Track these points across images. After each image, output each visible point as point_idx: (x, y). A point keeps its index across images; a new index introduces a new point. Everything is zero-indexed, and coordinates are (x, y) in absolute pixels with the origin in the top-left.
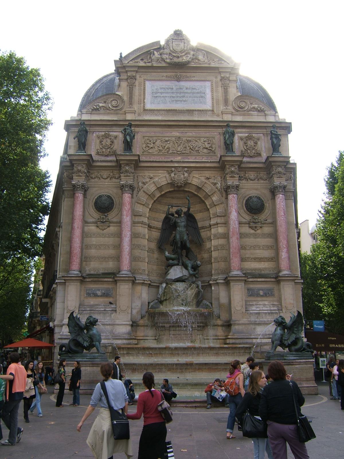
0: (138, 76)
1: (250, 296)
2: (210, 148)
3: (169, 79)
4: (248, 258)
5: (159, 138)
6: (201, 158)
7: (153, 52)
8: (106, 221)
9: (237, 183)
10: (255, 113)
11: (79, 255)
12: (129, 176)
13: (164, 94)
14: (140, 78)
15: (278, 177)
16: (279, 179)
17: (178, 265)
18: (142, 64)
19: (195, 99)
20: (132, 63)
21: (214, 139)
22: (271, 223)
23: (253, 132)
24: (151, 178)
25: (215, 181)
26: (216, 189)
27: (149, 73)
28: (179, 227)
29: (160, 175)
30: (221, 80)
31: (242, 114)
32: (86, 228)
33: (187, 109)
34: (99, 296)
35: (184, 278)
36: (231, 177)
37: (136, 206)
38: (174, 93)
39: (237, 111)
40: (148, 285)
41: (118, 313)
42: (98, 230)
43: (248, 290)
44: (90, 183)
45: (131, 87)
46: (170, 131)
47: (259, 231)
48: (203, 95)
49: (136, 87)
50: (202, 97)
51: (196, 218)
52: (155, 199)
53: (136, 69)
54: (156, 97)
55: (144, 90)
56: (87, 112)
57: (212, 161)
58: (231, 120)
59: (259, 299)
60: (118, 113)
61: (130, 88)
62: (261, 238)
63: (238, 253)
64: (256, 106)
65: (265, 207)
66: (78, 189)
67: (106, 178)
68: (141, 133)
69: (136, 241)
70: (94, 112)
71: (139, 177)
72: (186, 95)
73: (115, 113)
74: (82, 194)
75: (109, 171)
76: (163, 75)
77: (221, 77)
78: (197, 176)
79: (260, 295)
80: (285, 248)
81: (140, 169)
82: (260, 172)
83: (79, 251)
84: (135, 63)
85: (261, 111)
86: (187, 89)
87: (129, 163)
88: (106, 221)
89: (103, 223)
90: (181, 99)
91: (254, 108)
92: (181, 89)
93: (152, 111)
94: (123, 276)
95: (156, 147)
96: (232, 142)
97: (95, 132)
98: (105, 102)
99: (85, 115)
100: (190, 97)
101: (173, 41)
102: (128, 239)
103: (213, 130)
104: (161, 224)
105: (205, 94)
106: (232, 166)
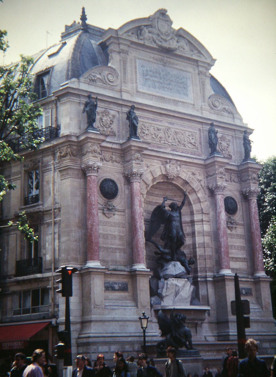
2: (195, 144)
5: (153, 125)
6: (187, 152)
14: (133, 54)
24: (148, 167)
28: (175, 221)
47: (234, 232)
48: (185, 86)
62: (236, 238)
64: (227, 107)
70: (92, 82)
88: (112, 209)
98: (100, 74)
99: (83, 84)
101: (159, 20)
106: (221, 167)
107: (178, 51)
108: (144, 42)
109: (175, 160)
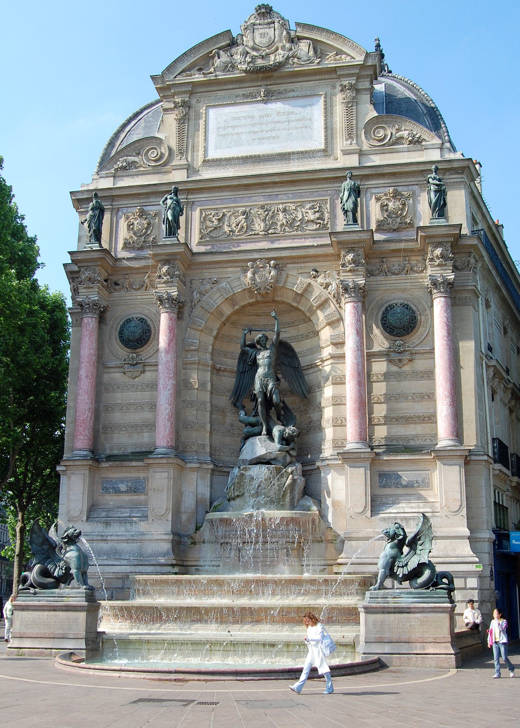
0: (194, 101)
1: (384, 487)
8: (137, 364)
11: (90, 423)
17: (260, 434)
18: (198, 77)
19: (294, 132)
20: (182, 79)
21: (326, 203)
22: (428, 351)
23: (400, 184)
24: (214, 283)
25: (327, 281)
26: (329, 295)
27: (213, 93)
29: (229, 276)
30: (342, 91)
32: (106, 377)
35: (268, 458)
36: (350, 271)
41: (150, 520)
42: (126, 379)
43: (380, 475)
44: (112, 299)
47: (406, 368)
48: (308, 123)
49: (190, 122)
50: (306, 127)
51: (296, 350)
54: (225, 135)
56: (108, 175)
57: (320, 243)
58: (357, 165)
65: (419, 322)
66: (87, 311)
67: (139, 289)
70: (120, 173)
71: (193, 282)
72: (278, 126)
73: (155, 171)
74: (94, 319)
76: (237, 93)
77: (341, 85)
79: (401, 484)
82: (411, 258)
83: (89, 416)
88: (137, 364)
89: (132, 367)
90: (268, 135)
91: (402, 138)
92: (267, 115)
93: (218, 163)
94: (159, 456)
97: (121, 209)
98: (138, 154)
100: (283, 129)
101: (256, 27)
102: (170, 392)
103: (325, 186)
104: (236, 361)
109: (264, 258)
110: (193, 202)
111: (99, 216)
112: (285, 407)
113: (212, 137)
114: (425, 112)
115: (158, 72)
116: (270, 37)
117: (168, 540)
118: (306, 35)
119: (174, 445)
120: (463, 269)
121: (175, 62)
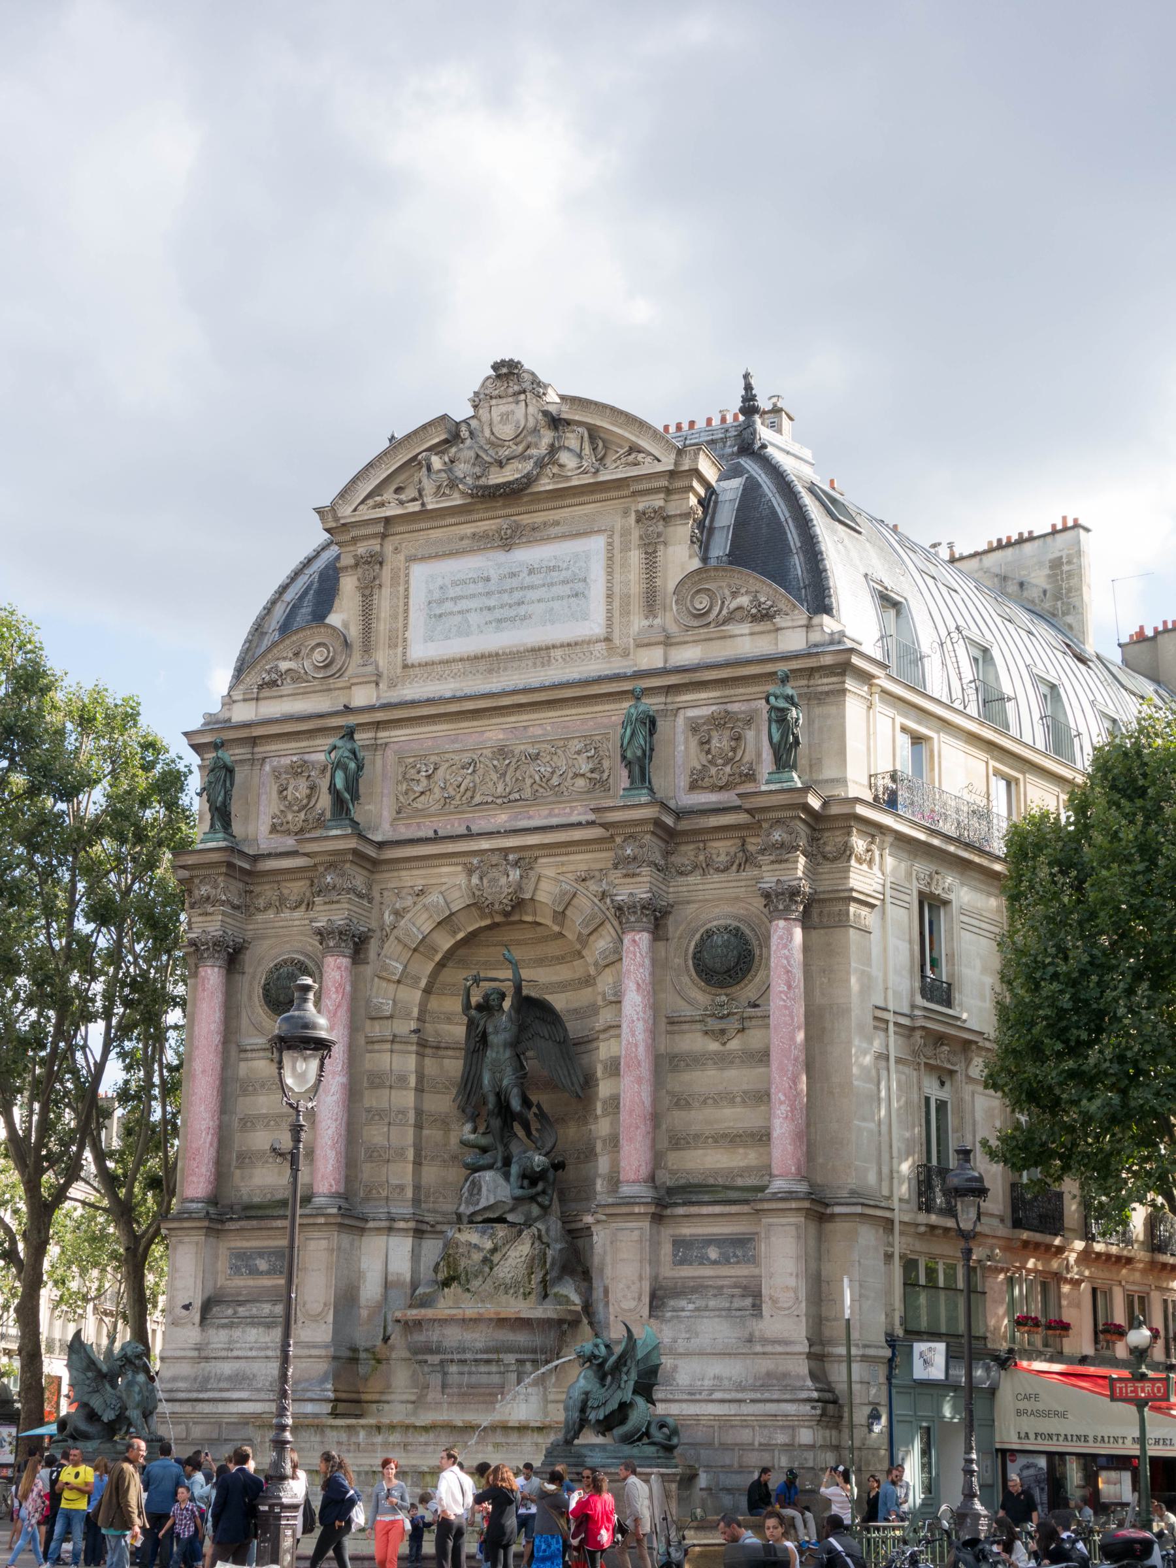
1: (682, 1262)
2: (594, 775)
3: (483, 543)
4: (697, 1136)
6: (568, 810)
7: (428, 459)
9: (644, 896)
10: (745, 628)
12: (337, 902)
13: (464, 601)
15: (773, 862)
16: (776, 866)
17: (490, 1167)
19: (556, 605)
20: (366, 513)
21: (609, 741)
23: (735, 699)
29: (443, 880)
30: (638, 521)
31: (703, 637)
33: (529, 646)
34: (261, 1273)
36: (626, 876)
37: (374, 990)
38: (493, 593)
39: (688, 628)
40: (411, 1234)
44: (251, 927)
45: (367, 592)
46: (479, 729)
47: (734, 1044)
48: (579, 586)
49: (383, 590)
52: (438, 958)
53: (380, 528)
54: (440, 616)
55: (407, 597)
58: (660, 664)
59: (707, 1271)
60: (332, 686)
61: (363, 596)
63: (637, 1128)
64: (744, 600)
65: (757, 959)
67: (296, 907)
68: (396, 747)
69: (372, 1099)
70: (266, 693)
71: (386, 893)
72: (532, 595)
73: (325, 687)
74: (216, 969)
75: (301, 883)
76: (462, 532)
77: (637, 511)
78: (550, 872)
79: (708, 1259)
80: (781, 1103)
81: (384, 867)
83: (208, 1140)
84: (374, 507)
85: (763, 616)
86: (531, 572)
87: (334, 862)
90: (512, 613)
91: (739, 608)
92: (513, 575)
95: (437, 790)
96: (639, 753)
98: (296, 654)
100: (539, 601)
101: (494, 402)
102: (335, 1098)
103: (607, 707)
105: (587, 584)
106: (632, 837)
107: (544, 480)
108: (423, 504)
110: (386, 744)
111: (225, 781)
112: (542, 1116)
113: (417, 617)
114: (799, 545)
115: (327, 502)
116: (518, 422)
117: (326, 1357)
118: (577, 418)
119: (342, 1191)
120: (835, 859)
121: (354, 481)
